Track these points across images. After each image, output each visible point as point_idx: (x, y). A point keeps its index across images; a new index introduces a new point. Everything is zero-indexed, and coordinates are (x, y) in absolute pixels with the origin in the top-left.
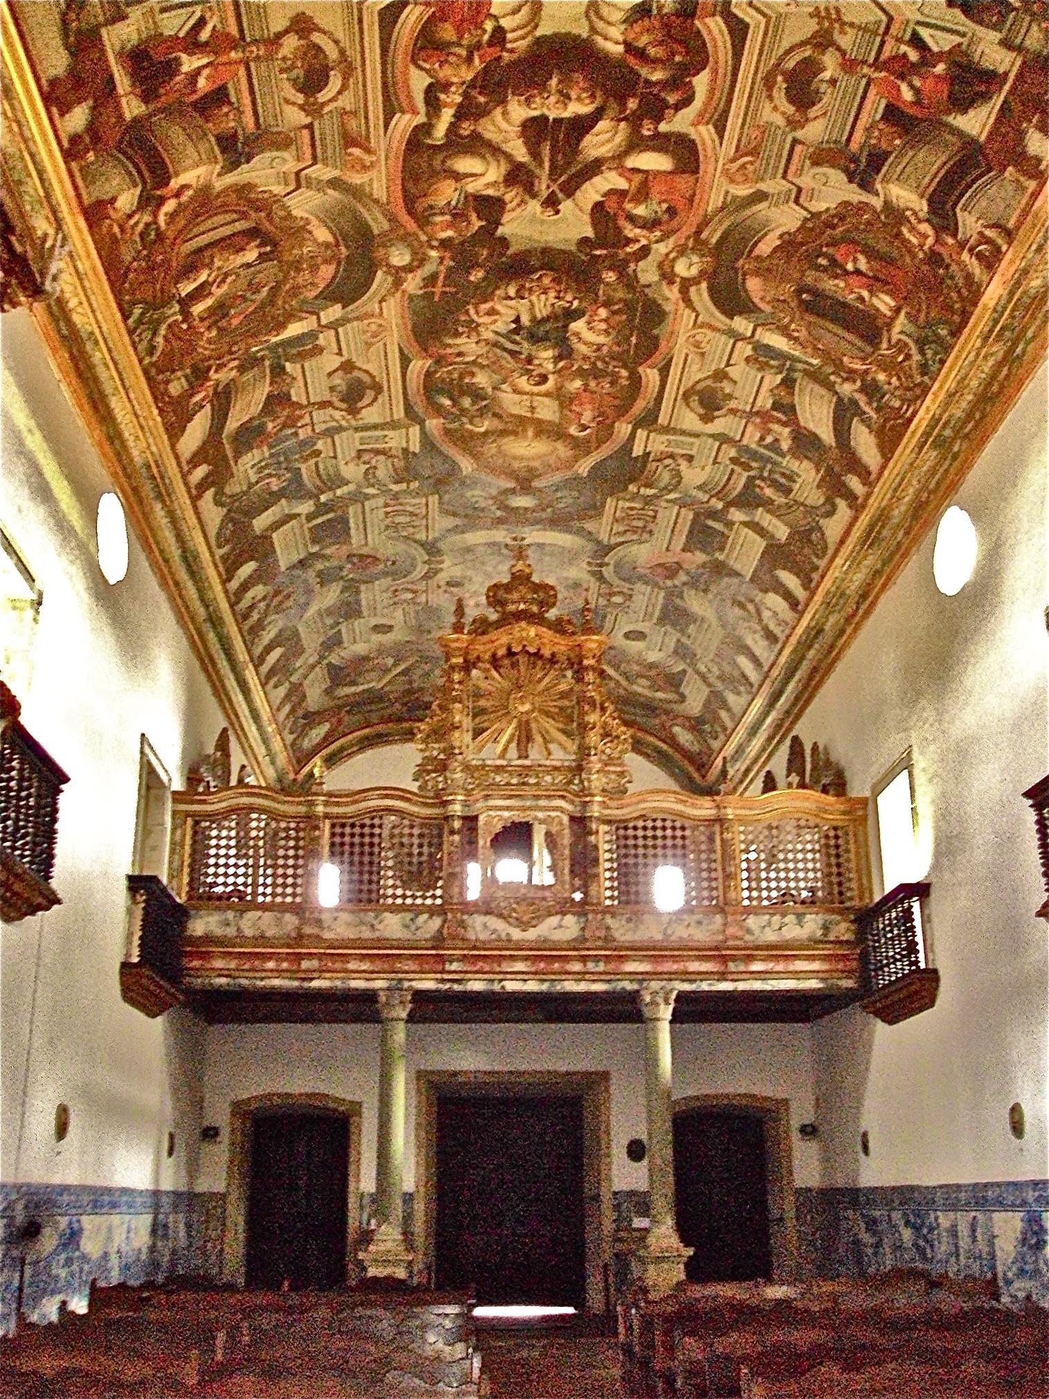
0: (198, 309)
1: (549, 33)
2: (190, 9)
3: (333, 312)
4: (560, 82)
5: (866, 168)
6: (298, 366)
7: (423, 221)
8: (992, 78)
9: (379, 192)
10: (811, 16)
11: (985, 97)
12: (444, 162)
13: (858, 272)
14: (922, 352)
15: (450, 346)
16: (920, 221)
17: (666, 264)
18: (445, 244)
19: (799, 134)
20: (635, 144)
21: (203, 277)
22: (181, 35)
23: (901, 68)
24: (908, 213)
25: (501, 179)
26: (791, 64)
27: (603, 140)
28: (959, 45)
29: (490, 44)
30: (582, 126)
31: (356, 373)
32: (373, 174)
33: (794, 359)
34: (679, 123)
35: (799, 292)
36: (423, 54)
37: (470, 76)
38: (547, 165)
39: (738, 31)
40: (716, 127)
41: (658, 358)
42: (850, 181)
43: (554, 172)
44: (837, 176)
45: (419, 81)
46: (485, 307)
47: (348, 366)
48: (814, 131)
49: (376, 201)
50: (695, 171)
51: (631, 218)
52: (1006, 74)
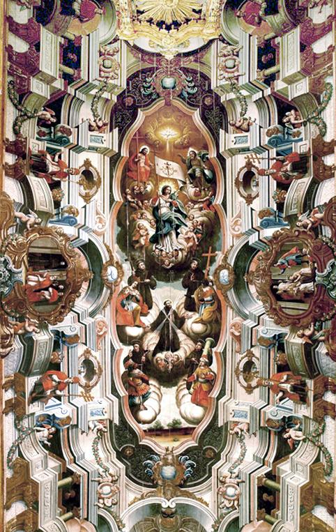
0: (307, 270)
1: (173, 388)
2: (283, 406)
3: (253, 239)
4: (168, 367)
5: (60, 340)
6: (271, 206)
7: (215, 297)
8: (33, 400)
9: (230, 311)
10: (93, 398)
11: (32, 393)
12: (206, 329)
13: (47, 289)
14: (10, 271)
15: (205, 215)
16: (34, 330)
17: (120, 273)
18: (206, 284)
19: (85, 348)
20: (140, 340)
21: (302, 286)
22: (288, 399)
23: (60, 386)
24: (38, 331)
26: (95, 377)
27: (152, 340)
29: (191, 383)
30: (160, 348)
31: (245, 194)
32: (232, 322)
35: (66, 266)
37: (198, 369)
38: (170, 328)
39: (114, 391)
40: (114, 349)
41: (116, 208)
42: (62, 332)
43: (167, 324)
44: (68, 332)
45: (214, 367)
46: (191, 244)
47: (249, 200)
48: (81, 349)
49: (232, 308)
50: (117, 326)
51: (138, 301)
52: (29, 405)
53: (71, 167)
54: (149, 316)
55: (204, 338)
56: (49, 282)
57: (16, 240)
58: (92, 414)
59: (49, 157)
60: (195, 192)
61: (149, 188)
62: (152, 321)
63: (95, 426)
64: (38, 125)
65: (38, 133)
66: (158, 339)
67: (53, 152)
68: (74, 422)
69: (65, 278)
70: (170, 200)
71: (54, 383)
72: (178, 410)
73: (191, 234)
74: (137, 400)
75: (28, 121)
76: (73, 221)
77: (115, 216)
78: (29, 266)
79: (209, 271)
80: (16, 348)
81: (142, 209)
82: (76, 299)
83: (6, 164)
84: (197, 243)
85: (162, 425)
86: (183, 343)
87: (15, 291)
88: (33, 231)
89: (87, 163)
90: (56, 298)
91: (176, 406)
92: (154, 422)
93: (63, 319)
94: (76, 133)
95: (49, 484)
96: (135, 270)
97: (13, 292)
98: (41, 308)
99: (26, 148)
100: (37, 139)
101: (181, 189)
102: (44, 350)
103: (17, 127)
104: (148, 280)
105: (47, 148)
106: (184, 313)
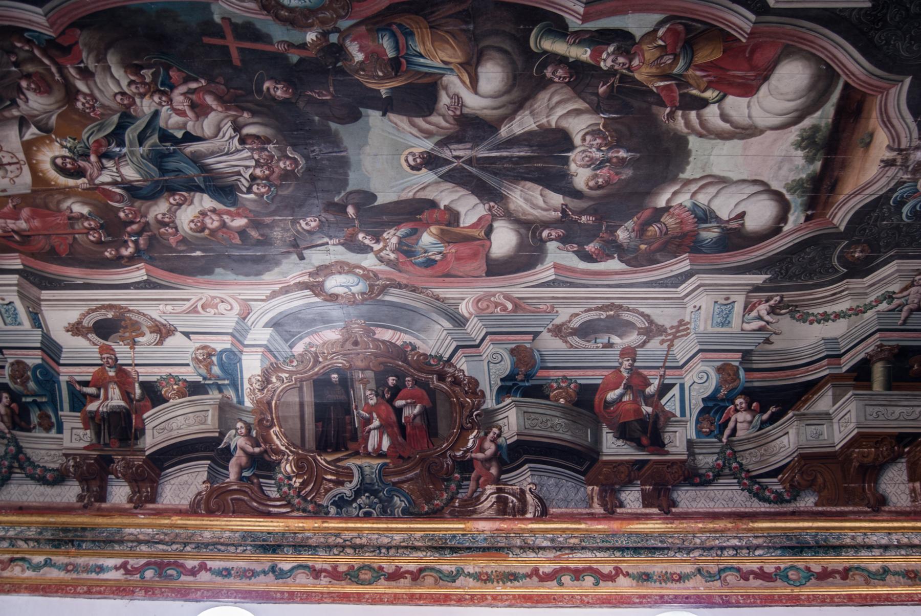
1: (690, 146)
4: (623, 160)
8: (657, 443)
11: (640, 446)
12: (501, 50)
13: (399, 411)
14: (358, 493)
15: (101, 59)
16: (493, 441)
18: (339, 51)
19: (546, 336)
24: (495, 430)
25: (465, 111)
26: (626, 316)
27: (531, 199)
28: (675, 416)
30: (556, 180)
33: (236, 385)
34: (558, 255)
36: (680, 28)
43: (485, 164)
46: (209, 100)
51: (415, 233)
52: (667, 453)
53: (100, 362)
54: (462, 208)
55: (530, 56)
56: (383, 407)
57: (290, 478)
58: (726, 322)
59: (92, 407)
60: (38, 91)
61: (80, 209)
62: (474, 200)
63: (760, 318)
64: (29, 430)
65: (48, 429)
66: (529, 184)
67: (78, 401)
68: (735, 359)
69: (370, 374)
70: (93, 158)
71: (626, 398)
72: (768, 133)
73: (178, 97)
74: (710, 234)
75: (29, 452)
76: (228, 357)
77: (190, 280)
78: (347, 449)
79: (290, 45)
80: (529, 480)
81: (147, 223)
82: (421, 351)
83: (130, 500)
84: (203, 82)
85: (804, 176)
86: (544, 121)
87: (404, 482)
88: (267, 440)
89: (76, 329)
90: (419, 391)
91: (753, 139)
92: (788, 197)
93: (471, 378)
94: (13, 352)
95: (869, 410)
96: (326, 240)
97: (405, 486)
98: (442, 426)
99: (86, 457)
100: (60, 430)
101: (45, 129)
102: (541, 418)
103: (48, 476)
104: (351, 210)
105: (73, 409)
106: (444, 116)
